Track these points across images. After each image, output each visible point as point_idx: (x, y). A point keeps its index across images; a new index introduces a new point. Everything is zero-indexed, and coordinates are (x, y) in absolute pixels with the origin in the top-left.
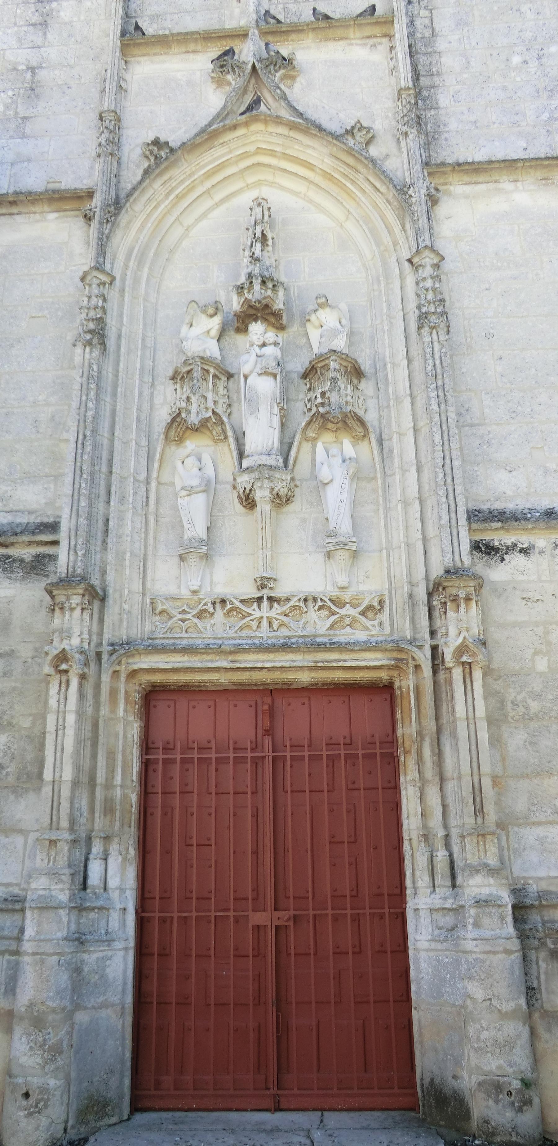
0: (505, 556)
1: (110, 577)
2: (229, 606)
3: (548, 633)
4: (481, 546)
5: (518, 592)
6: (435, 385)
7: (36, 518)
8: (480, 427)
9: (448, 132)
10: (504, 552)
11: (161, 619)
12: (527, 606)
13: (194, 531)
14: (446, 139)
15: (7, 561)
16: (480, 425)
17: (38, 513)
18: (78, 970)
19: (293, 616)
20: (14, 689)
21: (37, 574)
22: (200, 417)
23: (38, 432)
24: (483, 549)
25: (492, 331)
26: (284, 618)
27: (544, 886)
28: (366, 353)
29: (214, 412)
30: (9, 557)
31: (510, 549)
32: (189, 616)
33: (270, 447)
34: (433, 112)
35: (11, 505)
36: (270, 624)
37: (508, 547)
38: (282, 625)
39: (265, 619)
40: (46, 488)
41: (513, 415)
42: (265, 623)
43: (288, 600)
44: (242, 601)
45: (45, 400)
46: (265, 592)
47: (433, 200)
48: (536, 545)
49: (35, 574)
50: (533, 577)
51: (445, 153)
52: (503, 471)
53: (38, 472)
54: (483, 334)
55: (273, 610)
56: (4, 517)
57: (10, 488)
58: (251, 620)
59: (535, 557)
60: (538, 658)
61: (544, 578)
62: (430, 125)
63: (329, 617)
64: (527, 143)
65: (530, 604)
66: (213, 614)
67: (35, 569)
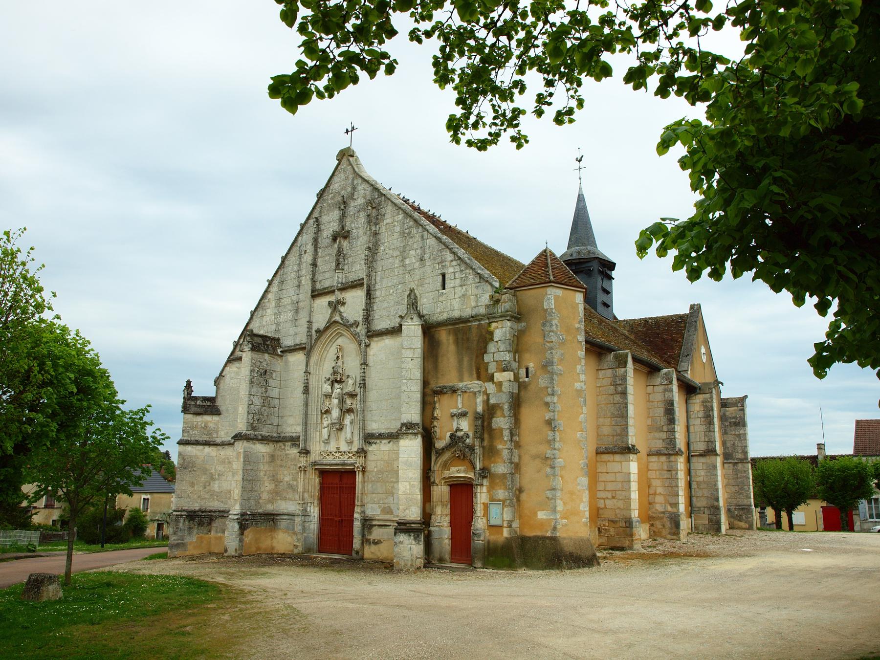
1: (311, 448)
18: (304, 526)
27: (371, 516)
47: (367, 346)
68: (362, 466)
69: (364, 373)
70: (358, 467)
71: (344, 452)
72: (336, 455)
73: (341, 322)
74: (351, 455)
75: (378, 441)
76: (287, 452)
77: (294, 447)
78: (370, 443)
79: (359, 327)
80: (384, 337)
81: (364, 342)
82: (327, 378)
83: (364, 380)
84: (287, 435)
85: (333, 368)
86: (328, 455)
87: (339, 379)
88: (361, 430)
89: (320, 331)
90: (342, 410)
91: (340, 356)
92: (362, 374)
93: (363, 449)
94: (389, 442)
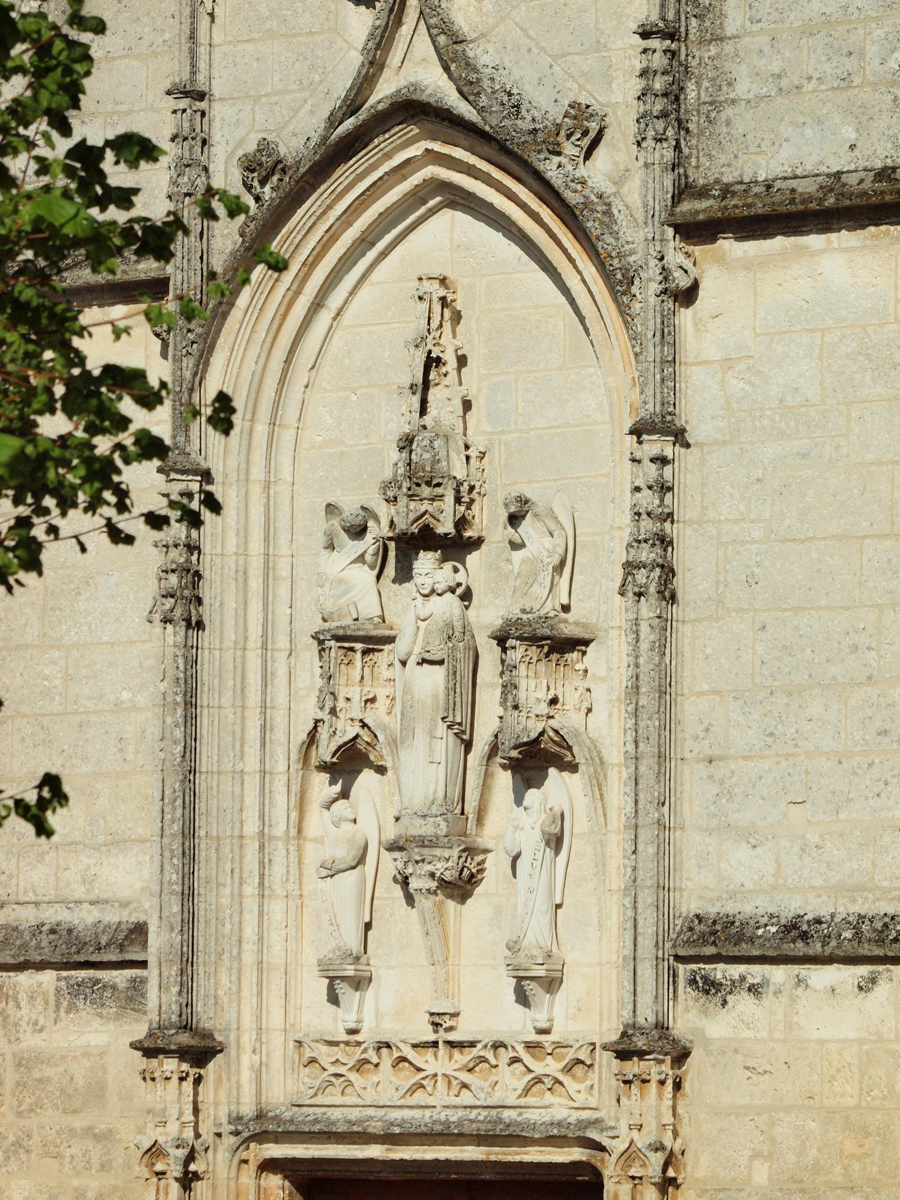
0: (729, 998)
1: (230, 1015)
2: (396, 1054)
3: (773, 1124)
4: (698, 978)
5: (739, 1058)
6: (633, 706)
7: (130, 914)
8: (721, 763)
9: (733, 102)
10: (728, 989)
11: (312, 1072)
12: (750, 1081)
13: (339, 936)
14: (728, 123)
15: (95, 988)
16: (721, 758)
17: (132, 906)
19: (481, 1071)
20: (115, 1188)
21: (133, 1009)
22: (339, 740)
23: (125, 760)
24: (701, 985)
25: (757, 571)
26: (465, 1077)
28: (601, 588)
29: (364, 725)
30: (98, 981)
31: (736, 985)
32: (342, 1070)
33: (432, 798)
34: (713, 50)
35: (97, 891)
36: (450, 1082)
37: (733, 982)
38: (465, 1086)
39: (439, 1078)
40: (140, 863)
41: (770, 740)
42: (441, 1083)
43: (472, 1044)
44: (414, 1046)
45: (131, 700)
46: (442, 1036)
48: (772, 980)
49: (132, 1009)
50: (764, 1034)
51: (723, 159)
52: (744, 845)
53: (129, 833)
54: (743, 577)
55: (453, 1062)
56: (89, 912)
57: (93, 861)
58: (423, 1079)
59: (768, 998)
60: (757, 1163)
61: (777, 1035)
62: (706, 84)
63: (525, 1074)
64: (857, 130)
65: (754, 1077)
66: (377, 1065)
67: (131, 1001)
68: (659, 1147)
69: (664, 488)
70: (630, 1155)
71: (497, 1046)
72: (430, 1062)
73: (463, 109)
74: (551, 1066)
75: (778, 974)
76: (31, 1041)
77: (86, 1011)
78: (709, 987)
79: (601, 152)
80: (815, 241)
81: (653, 270)
82: (350, 506)
83: (664, 542)
84: (27, 916)
85: (407, 443)
86: (362, 1065)
87: (445, 527)
88: (647, 898)
89: (278, 166)
90: (468, 746)
91: (450, 359)
92: (648, 500)
93: (661, 1027)
94: (866, 986)
